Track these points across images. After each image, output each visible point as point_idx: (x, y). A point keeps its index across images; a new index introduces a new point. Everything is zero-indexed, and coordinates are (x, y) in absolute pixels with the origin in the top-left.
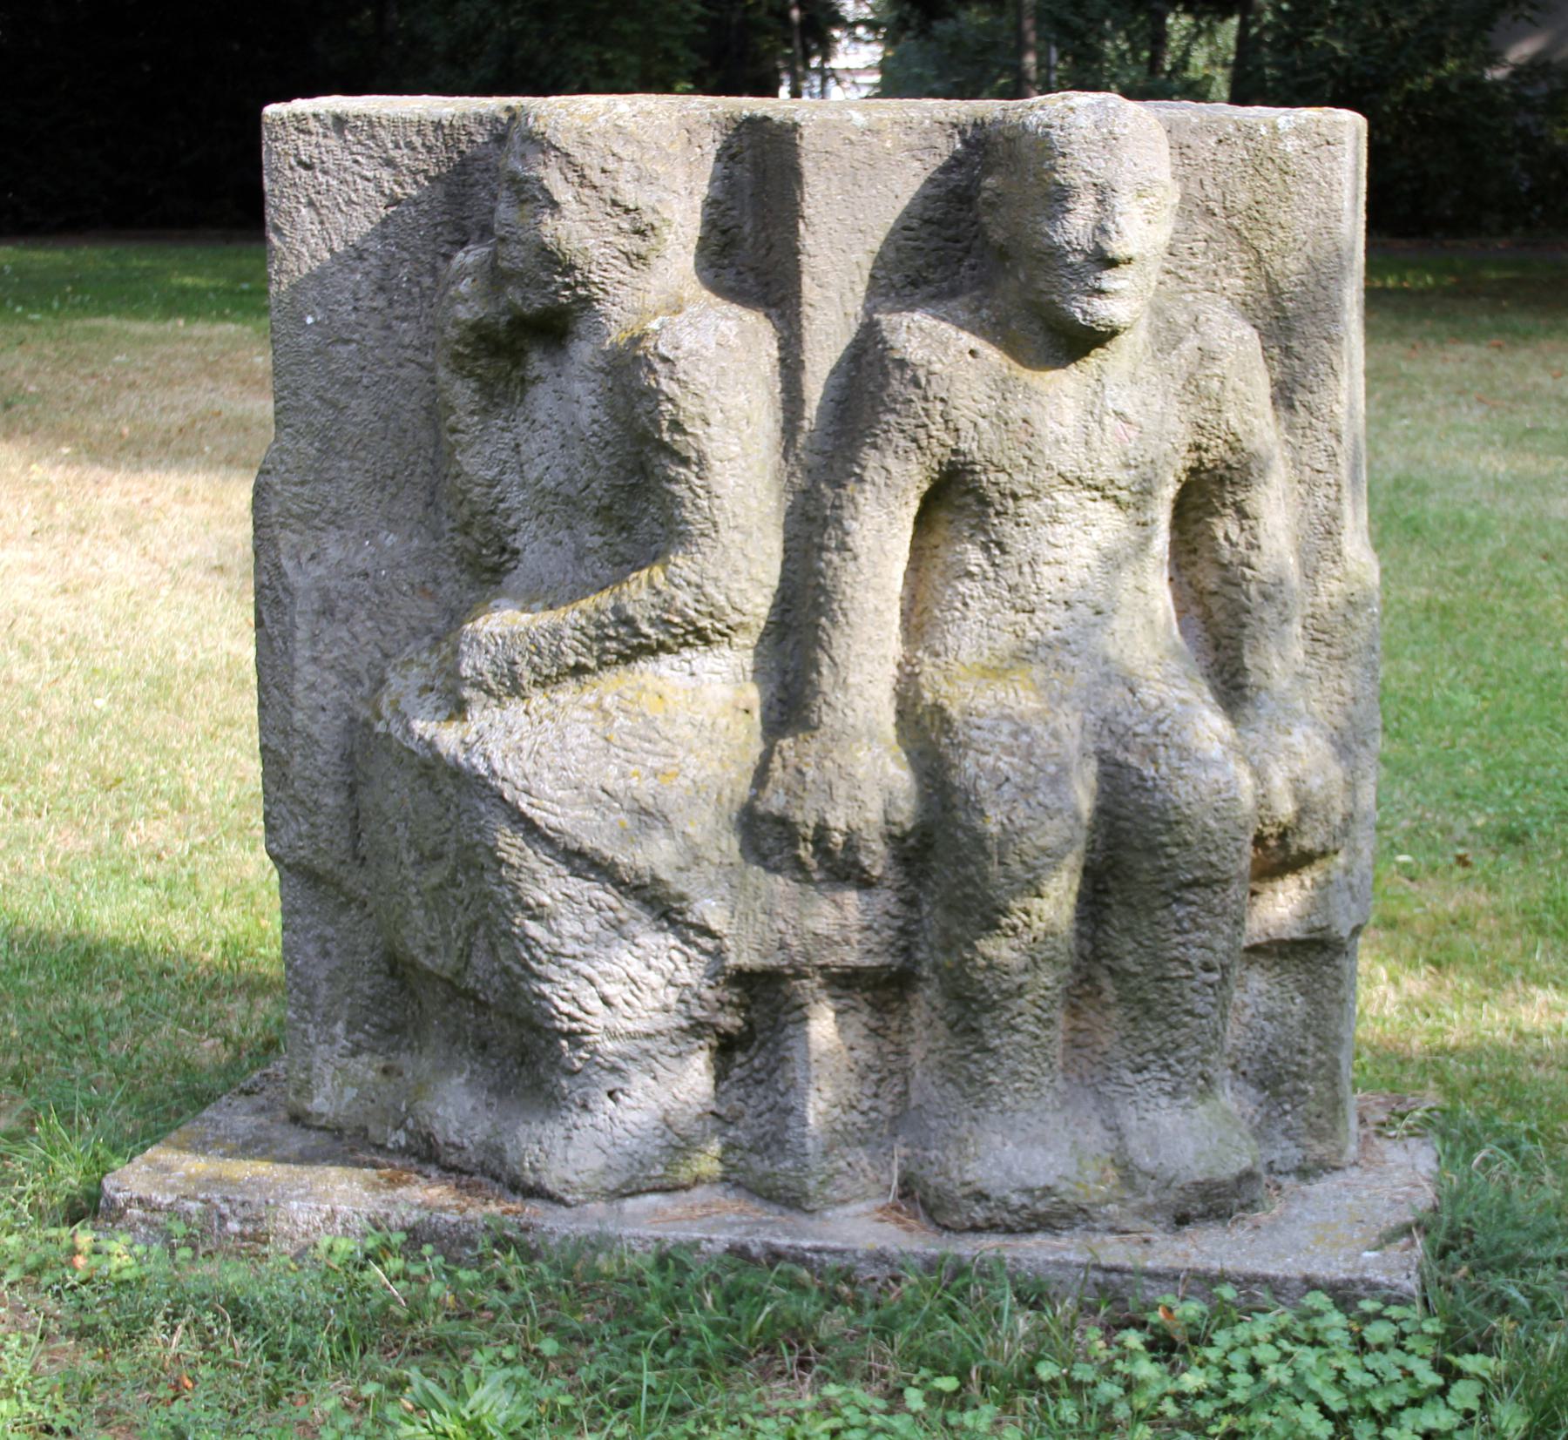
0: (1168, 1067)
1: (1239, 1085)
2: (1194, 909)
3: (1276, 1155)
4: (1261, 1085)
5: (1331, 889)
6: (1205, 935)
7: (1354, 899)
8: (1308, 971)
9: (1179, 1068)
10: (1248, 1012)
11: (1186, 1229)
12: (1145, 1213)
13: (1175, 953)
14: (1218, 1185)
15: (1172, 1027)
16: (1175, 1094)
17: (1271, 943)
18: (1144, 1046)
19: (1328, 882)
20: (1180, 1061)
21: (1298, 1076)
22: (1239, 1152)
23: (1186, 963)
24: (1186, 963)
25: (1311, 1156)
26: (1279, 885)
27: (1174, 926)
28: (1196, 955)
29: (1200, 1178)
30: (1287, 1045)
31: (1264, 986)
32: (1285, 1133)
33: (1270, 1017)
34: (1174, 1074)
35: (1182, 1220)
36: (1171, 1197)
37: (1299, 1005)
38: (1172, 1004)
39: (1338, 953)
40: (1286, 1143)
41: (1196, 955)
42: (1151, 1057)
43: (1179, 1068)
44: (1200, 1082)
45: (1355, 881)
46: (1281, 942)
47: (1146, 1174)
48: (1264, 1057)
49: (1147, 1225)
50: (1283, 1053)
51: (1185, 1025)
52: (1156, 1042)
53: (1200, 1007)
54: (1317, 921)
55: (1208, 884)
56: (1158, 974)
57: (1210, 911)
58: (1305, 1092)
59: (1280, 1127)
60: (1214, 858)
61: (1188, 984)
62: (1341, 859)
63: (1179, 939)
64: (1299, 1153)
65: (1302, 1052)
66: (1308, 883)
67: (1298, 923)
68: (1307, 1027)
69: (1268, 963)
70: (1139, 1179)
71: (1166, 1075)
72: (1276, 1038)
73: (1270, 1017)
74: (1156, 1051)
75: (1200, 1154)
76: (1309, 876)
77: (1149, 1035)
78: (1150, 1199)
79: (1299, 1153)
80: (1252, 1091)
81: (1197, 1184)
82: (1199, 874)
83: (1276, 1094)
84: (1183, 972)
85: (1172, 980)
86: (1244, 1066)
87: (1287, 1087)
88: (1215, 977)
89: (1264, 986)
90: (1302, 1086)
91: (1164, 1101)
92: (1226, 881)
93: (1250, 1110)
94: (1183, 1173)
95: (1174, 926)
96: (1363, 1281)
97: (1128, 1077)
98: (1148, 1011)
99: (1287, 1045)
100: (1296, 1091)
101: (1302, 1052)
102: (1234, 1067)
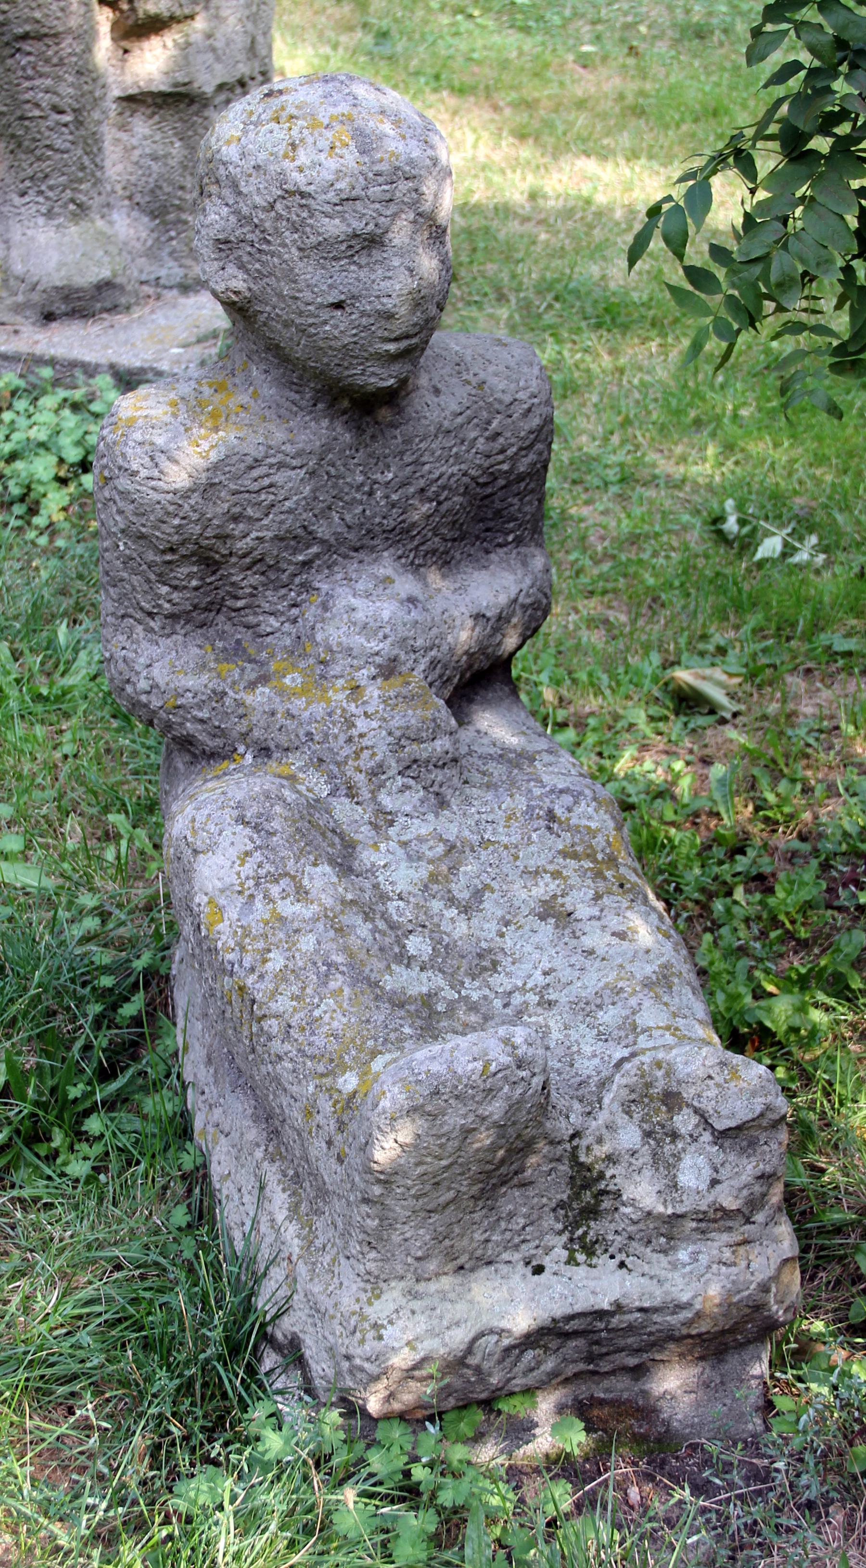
0: (40, 193)
1: (135, 214)
2: (32, 59)
3: (163, 273)
4: (153, 215)
5: (190, 50)
6: (49, 82)
7: (218, 59)
8: (181, 119)
9: (50, 194)
10: (137, 153)
11: (54, 325)
12: (18, 309)
13: (27, 96)
14: (78, 290)
15: (39, 159)
16: (49, 215)
17: (142, 94)
18: (22, 175)
19: (188, 44)
20: (51, 188)
21: (180, 208)
22: (99, 264)
23: (37, 105)
24: (37, 105)
25: (191, 274)
26: (146, 45)
27: (20, 73)
28: (45, 99)
29: (59, 283)
30: (171, 182)
31: (147, 131)
32: (171, 254)
33: (155, 158)
34: (47, 198)
35: (49, 317)
36: (36, 297)
37: (177, 149)
38: (35, 140)
39: (205, 106)
40: (171, 263)
41: (45, 99)
42: (28, 183)
43: (50, 194)
44: (72, 207)
45: (219, 44)
46: (151, 94)
47: (17, 278)
48: (152, 191)
49: (19, 319)
50: (167, 189)
51: (49, 158)
52: (30, 172)
53: (59, 143)
54: (181, 77)
55: (39, 37)
56: (18, 113)
57: (47, 61)
58: (186, 222)
59: (167, 250)
60: (37, 15)
61: (44, 124)
62: (200, 24)
63: (27, 84)
64: (181, 272)
65: (182, 188)
66: (170, 44)
67: (164, 79)
68: (185, 168)
69: (149, 112)
70: (12, 282)
71: (41, 199)
72: (161, 176)
73: (155, 158)
74: (32, 178)
75: (61, 265)
76: (170, 39)
77: (25, 165)
78: (20, 298)
79: (181, 272)
80: (146, 219)
81: (56, 288)
82: (28, 28)
83: (164, 223)
84: (37, 113)
85: (30, 119)
86: (138, 198)
87: (172, 217)
88: (67, 118)
89: (147, 131)
90: (184, 216)
91: (41, 221)
92: (55, 35)
93: (144, 235)
94: (45, 280)
95: (20, 73)
96: (152, 369)
97: (17, 200)
98: (20, 145)
99: (171, 182)
100: (179, 221)
101: (182, 188)
102: (130, 198)
